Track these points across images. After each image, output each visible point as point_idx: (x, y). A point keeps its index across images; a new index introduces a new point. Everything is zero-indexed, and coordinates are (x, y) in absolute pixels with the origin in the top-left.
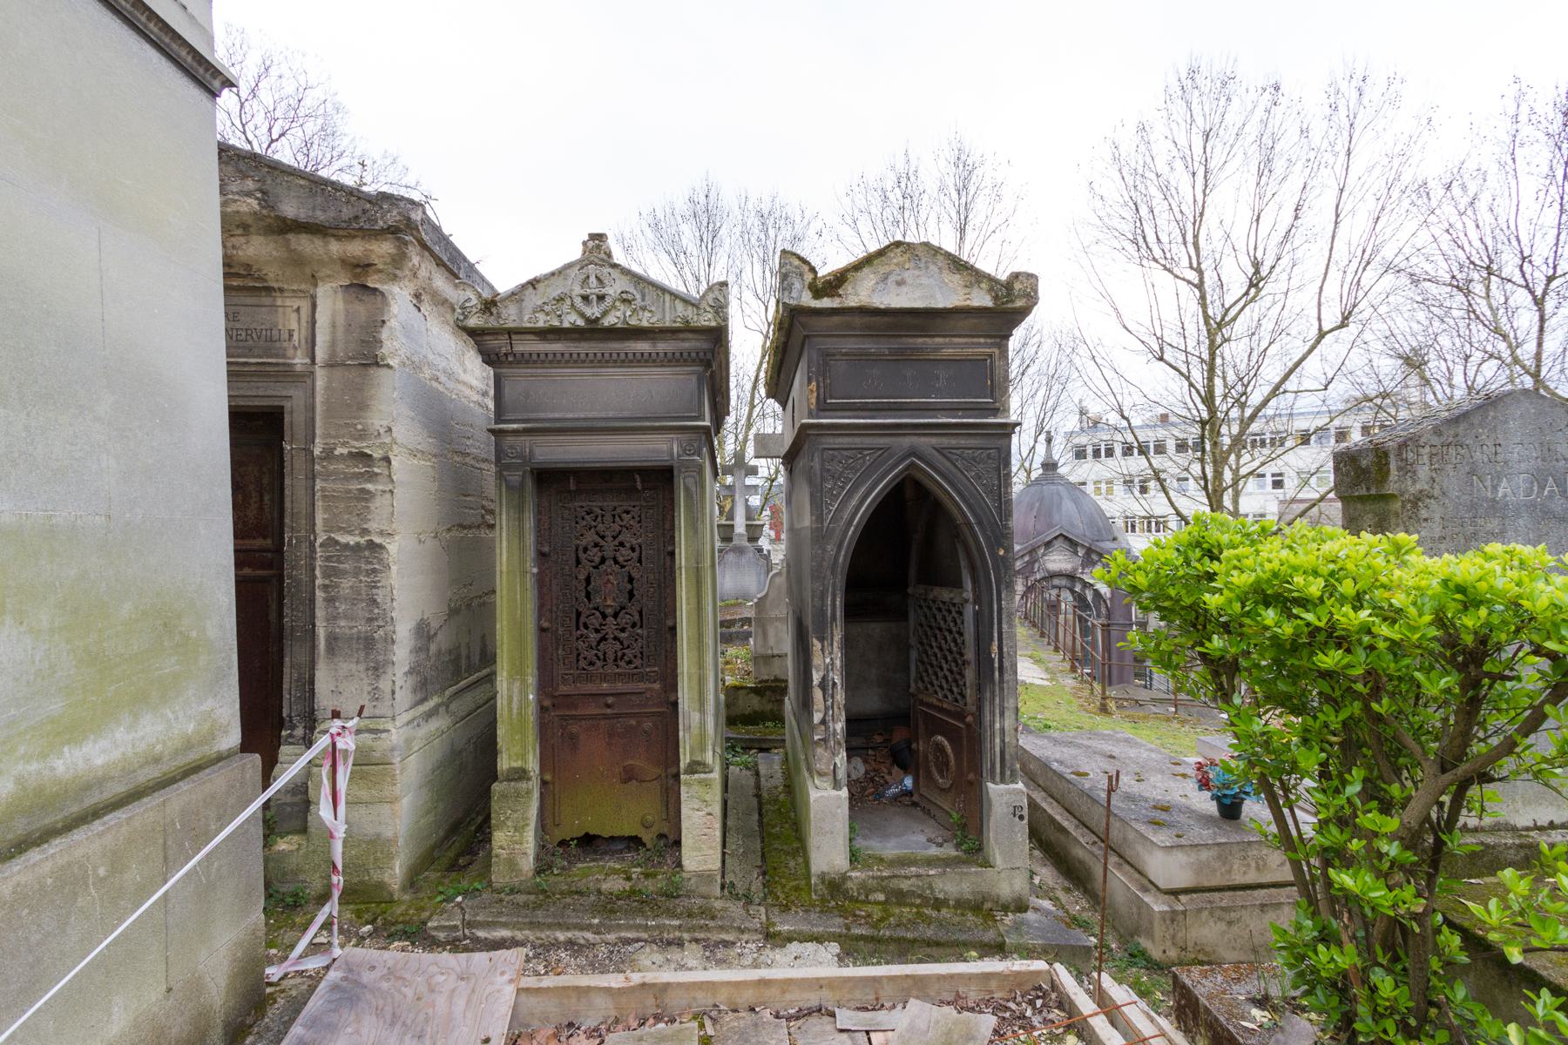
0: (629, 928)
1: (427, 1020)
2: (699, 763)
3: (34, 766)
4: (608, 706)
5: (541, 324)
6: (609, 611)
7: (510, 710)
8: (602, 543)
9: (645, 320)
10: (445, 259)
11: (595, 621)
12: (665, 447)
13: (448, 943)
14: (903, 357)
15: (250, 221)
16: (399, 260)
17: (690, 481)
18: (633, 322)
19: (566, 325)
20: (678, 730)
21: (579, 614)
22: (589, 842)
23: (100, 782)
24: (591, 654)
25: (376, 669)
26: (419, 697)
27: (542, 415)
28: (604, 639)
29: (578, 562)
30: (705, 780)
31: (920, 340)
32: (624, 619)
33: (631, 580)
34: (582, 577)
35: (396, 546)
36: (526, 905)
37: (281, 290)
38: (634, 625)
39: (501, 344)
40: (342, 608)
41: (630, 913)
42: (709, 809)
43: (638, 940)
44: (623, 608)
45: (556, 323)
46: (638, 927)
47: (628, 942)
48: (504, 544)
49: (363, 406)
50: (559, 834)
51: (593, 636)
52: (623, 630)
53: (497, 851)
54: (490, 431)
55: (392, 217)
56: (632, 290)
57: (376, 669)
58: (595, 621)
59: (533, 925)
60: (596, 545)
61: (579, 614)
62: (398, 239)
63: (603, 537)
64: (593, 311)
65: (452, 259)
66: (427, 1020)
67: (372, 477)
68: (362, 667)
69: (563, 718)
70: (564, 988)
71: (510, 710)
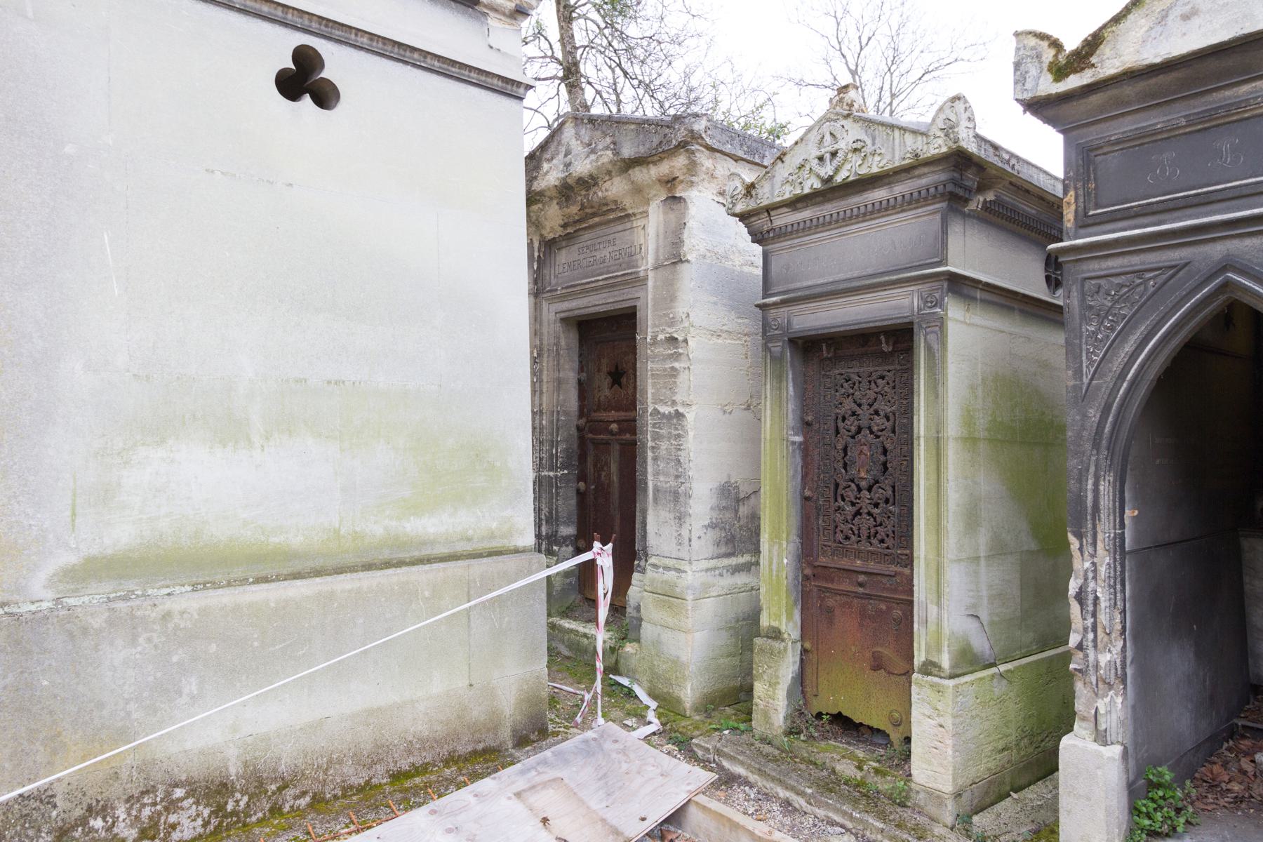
0: (837, 811)
1: (621, 788)
2: (934, 664)
3: (394, 523)
4: (861, 585)
5: (787, 196)
6: (863, 484)
7: (771, 570)
8: (859, 411)
9: (875, 166)
10: (741, 154)
11: (851, 494)
12: (906, 302)
13: (704, 761)
14: (1210, 124)
15: (610, 167)
16: (692, 167)
17: (931, 337)
18: (864, 171)
19: (807, 191)
20: (912, 622)
21: (837, 485)
22: (844, 724)
23: (433, 543)
24: (845, 528)
25: (680, 519)
26: (723, 550)
27: (798, 285)
28: (858, 513)
29: (837, 432)
30: (938, 685)
31: (1245, 88)
32: (878, 494)
33: (885, 452)
34: (840, 447)
35: (711, 419)
36: (767, 755)
37: (634, 214)
38: (887, 501)
39: (762, 222)
40: (662, 465)
41: (843, 798)
42: (941, 720)
43: (842, 826)
44: (877, 482)
45: (798, 191)
46: (844, 813)
47: (833, 823)
48: (768, 412)
49: (673, 298)
50: (817, 706)
51: (849, 508)
52: (876, 505)
53: (756, 700)
54: (757, 306)
55: (681, 135)
56: (864, 137)
57: (680, 519)
58: (851, 494)
59: (761, 772)
60: (854, 414)
61: (837, 485)
62: (687, 151)
63: (860, 405)
64: (827, 170)
65: (752, 151)
66: (621, 788)
67: (677, 356)
68: (672, 516)
69: (820, 589)
70: (721, 815)
71: (771, 570)
